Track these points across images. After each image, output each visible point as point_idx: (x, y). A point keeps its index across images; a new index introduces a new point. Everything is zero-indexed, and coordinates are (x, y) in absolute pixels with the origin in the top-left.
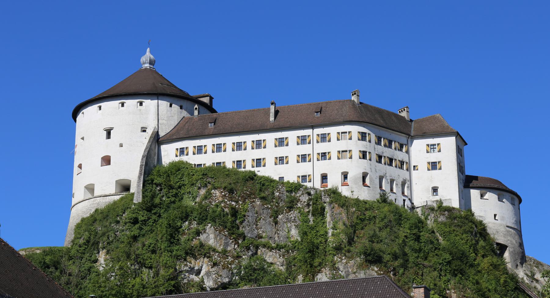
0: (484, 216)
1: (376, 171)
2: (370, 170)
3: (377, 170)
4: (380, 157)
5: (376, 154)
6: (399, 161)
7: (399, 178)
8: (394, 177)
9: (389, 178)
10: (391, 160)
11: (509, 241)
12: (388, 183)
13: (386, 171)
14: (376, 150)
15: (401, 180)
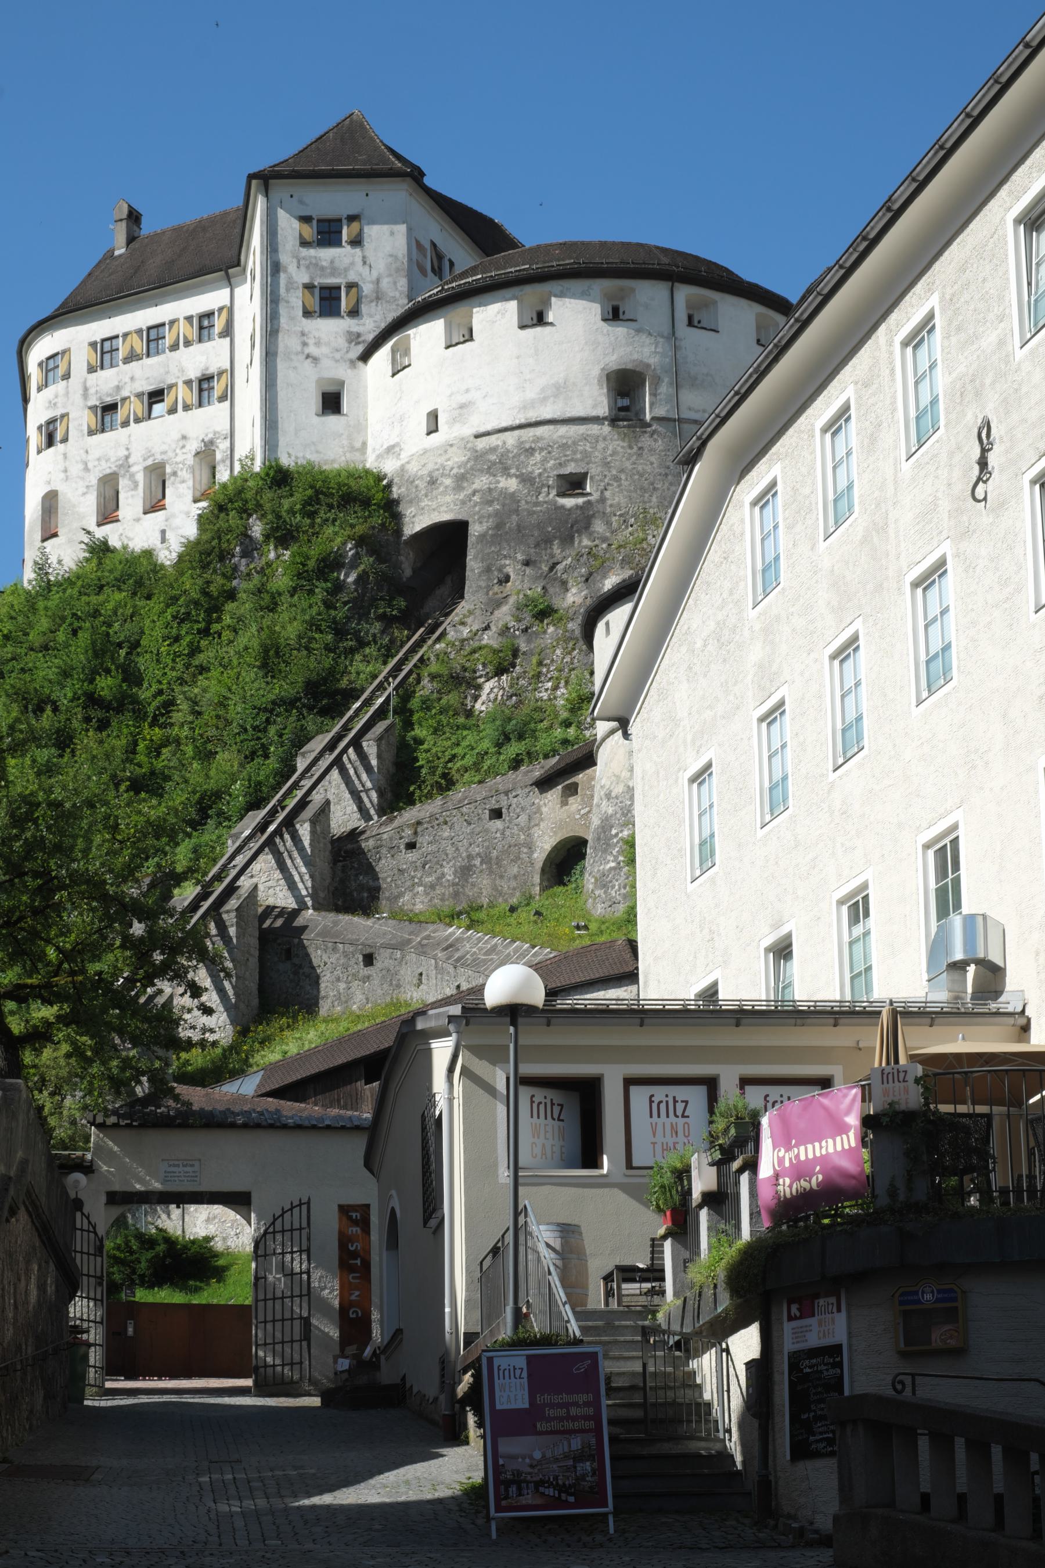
0: (397, 440)
1: (87, 469)
2: (62, 475)
3: (90, 465)
4: (110, 408)
5: (90, 408)
6: (188, 383)
7: (183, 447)
8: (164, 453)
9: (138, 470)
10: (156, 396)
11: (476, 498)
12: (136, 485)
13: (128, 449)
14: (92, 391)
15: (194, 446)
